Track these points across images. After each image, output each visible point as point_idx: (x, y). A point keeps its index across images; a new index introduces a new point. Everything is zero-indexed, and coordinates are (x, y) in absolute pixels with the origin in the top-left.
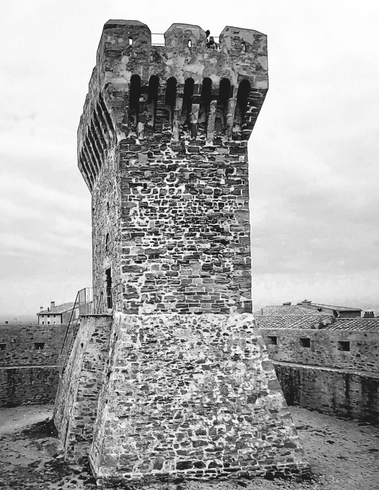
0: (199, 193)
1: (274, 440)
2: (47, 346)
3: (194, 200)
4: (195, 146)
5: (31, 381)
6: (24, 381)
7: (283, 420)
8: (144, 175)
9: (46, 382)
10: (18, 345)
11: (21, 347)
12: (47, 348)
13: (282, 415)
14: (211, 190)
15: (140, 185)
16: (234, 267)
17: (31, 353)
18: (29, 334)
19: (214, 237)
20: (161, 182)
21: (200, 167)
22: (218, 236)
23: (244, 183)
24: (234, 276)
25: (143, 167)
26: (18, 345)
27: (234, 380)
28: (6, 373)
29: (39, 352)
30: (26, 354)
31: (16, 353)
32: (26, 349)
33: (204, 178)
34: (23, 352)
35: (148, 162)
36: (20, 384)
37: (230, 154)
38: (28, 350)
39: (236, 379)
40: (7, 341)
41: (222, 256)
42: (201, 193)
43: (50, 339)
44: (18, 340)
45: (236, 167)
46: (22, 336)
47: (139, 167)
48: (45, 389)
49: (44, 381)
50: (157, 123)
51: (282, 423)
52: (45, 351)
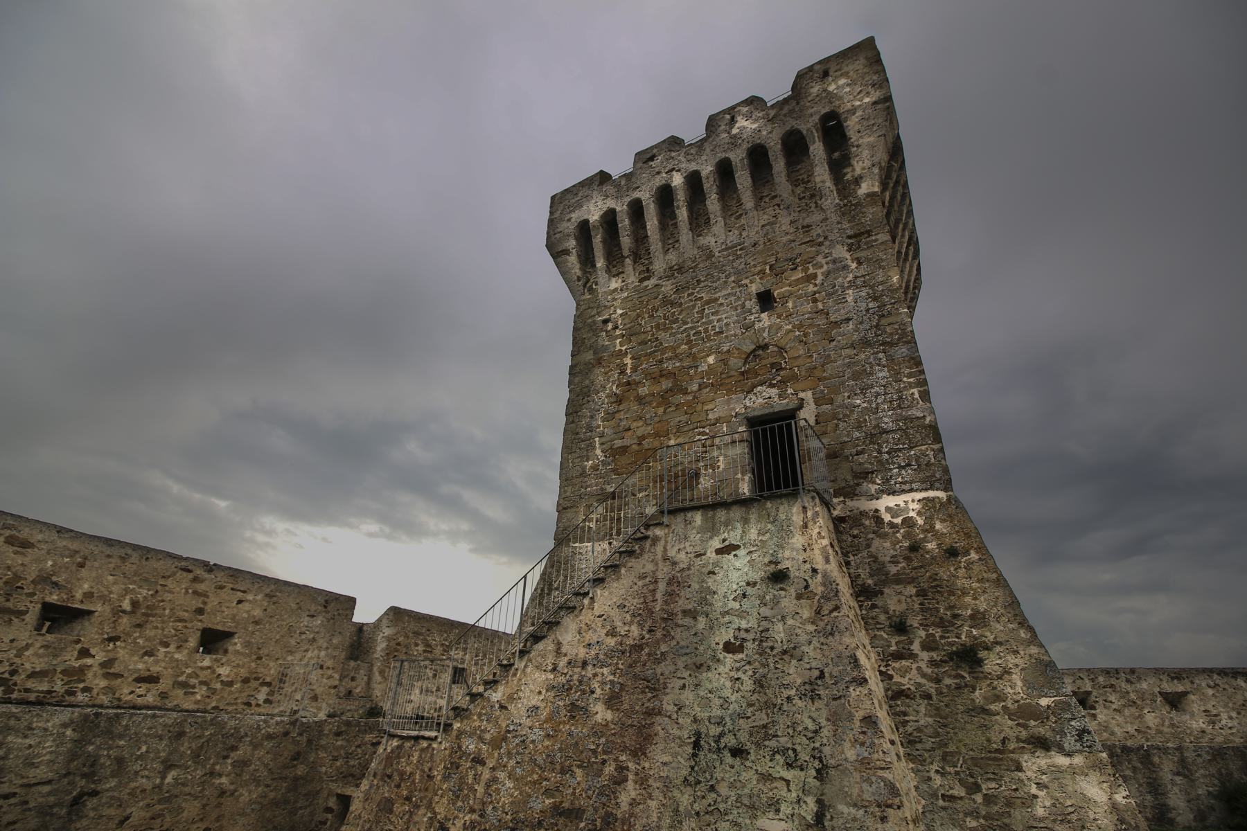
2: (239, 647)
5: (168, 766)
6: (136, 773)
9: (220, 775)
10: (139, 626)
11: (152, 633)
12: (237, 652)
17: (177, 660)
18: (195, 593)
26: (139, 626)
28: (69, 732)
29: (207, 663)
30: (157, 662)
31: (122, 653)
32: (167, 645)
34: (149, 653)
36: (113, 783)
38: (172, 648)
40: (104, 599)
43: (256, 623)
44: (148, 607)
46: (168, 597)
48: (204, 806)
49: (212, 774)
52: (228, 663)
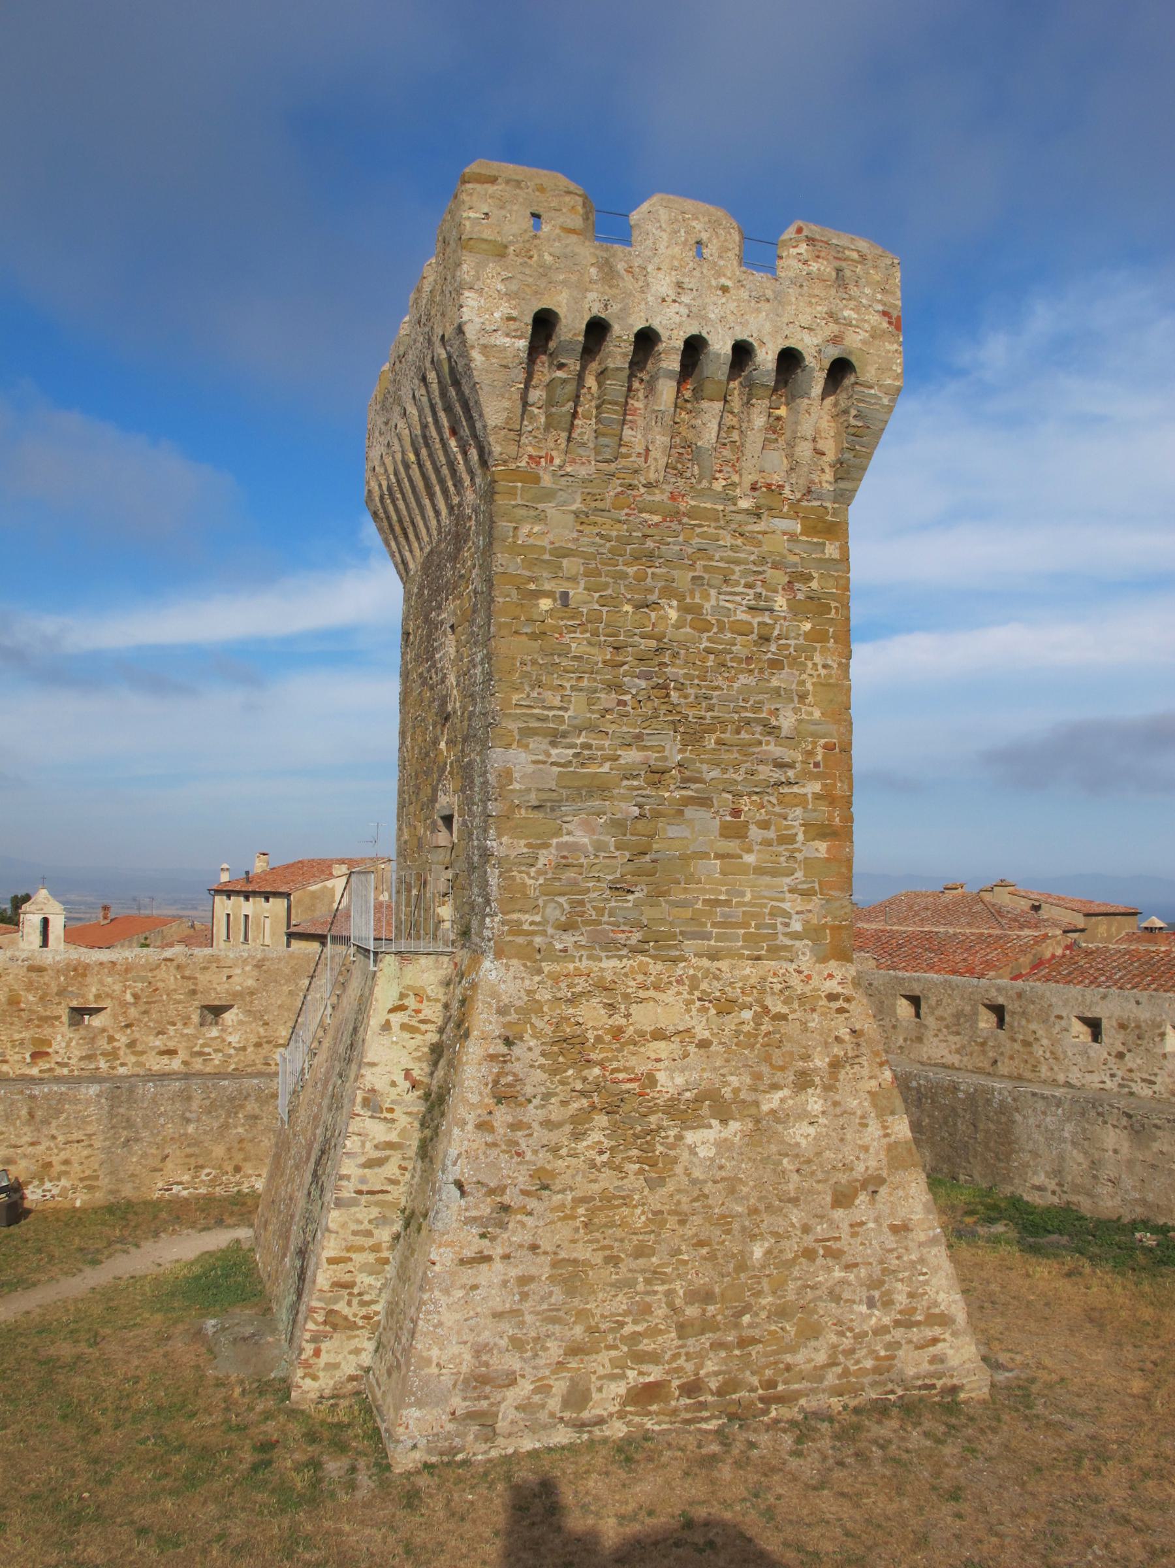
0: (715, 630)
1: (898, 1307)
3: (702, 646)
4: (708, 505)
7: (925, 1251)
8: (560, 568)
13: (922, 1237)
14: (750, 623)
15: (549, 594)
16: (805, 832)
19: (757, 750)
20: (609, 592)
21: (721, 559)
22: (764, 748)
23: (837, 613)
24: (806, 858)
25: (561, 547)
27: (798, 1144)
33: (728, 589)
35: (575, 535)
37: (801, 534)
39: (804, 1143)
41: (775, 802)
42: (721, 630)
45: (818, 569)
47: (549, 547)
50: (604, 435)
51: (922, 1261)
